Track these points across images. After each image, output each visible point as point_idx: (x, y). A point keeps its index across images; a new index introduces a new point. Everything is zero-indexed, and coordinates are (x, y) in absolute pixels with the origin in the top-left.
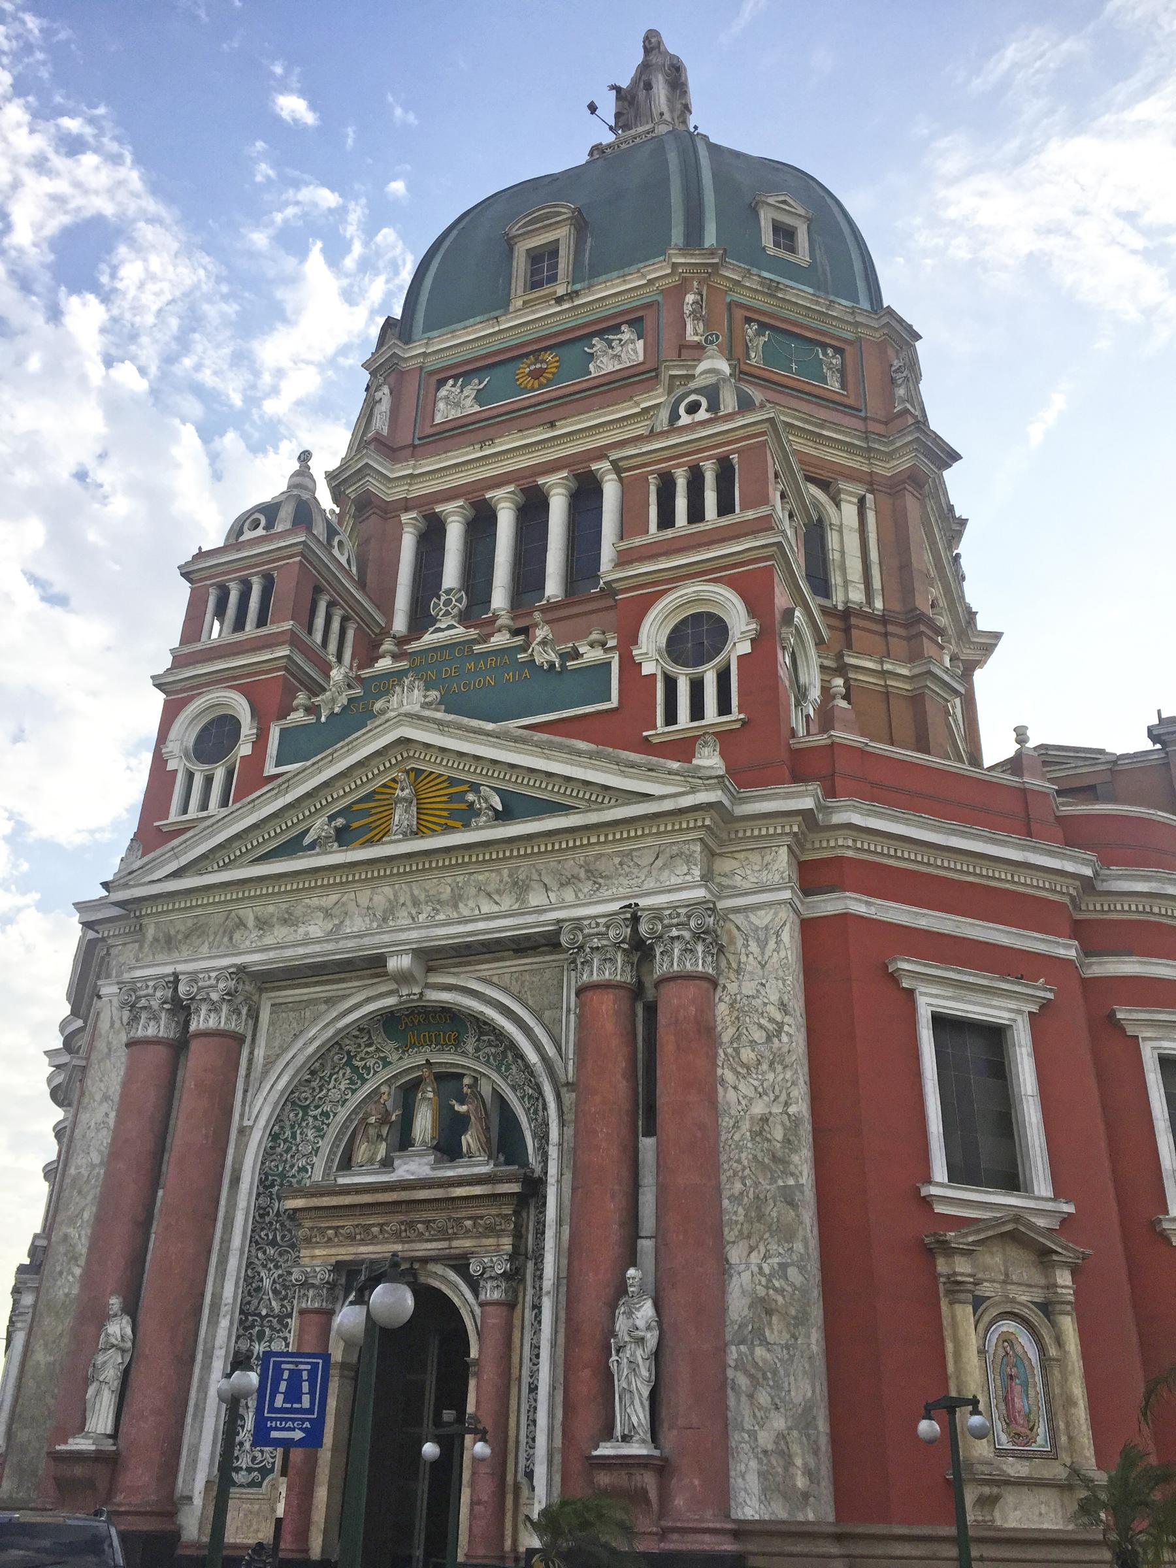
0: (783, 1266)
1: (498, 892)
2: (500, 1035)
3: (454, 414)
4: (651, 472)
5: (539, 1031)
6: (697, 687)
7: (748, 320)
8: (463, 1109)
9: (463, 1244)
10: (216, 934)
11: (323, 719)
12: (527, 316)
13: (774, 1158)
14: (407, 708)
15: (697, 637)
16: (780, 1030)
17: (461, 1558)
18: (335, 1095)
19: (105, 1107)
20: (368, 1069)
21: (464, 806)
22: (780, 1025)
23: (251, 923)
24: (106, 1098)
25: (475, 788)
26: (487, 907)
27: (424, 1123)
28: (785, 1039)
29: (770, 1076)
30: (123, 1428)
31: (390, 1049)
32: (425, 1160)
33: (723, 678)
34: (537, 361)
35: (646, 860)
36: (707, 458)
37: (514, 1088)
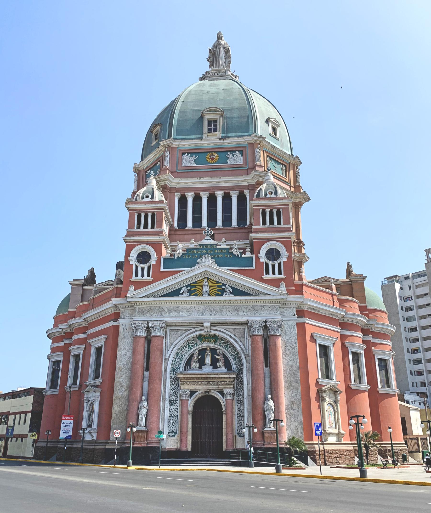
0: (296, 395)
1: (231, 311)
2: (227, 341)
3: (188, 165)
4: (261, 209)
5: (239, 342)
6: (273, 266)
7: (268, 156)
8: (218, 357)
9: (221, 387)
10: (156, 312)
11: (176, 258)
12: (210, 140)
13: (294, 374)
14: (206, 263)
15: (273, 254)
16: (295, 348)
17: (223, 450)
18: (184, 351)
19: (125, 351)
20: (192, 346)
21: (221, 289)
22: (295, 347)
23: (166, 310)
24: (125, 348)
25: (225, 285)
26: (229, 314)
27: (208, 360)
28: (296, 349)
29: (293, 357)
30: (147, 424)
31: (198, 342)
32: (210, 368)
33: (280, 265)
34: (212, 155)
35: (267, 308)
36: (275, 208)
37: (229, 353)
